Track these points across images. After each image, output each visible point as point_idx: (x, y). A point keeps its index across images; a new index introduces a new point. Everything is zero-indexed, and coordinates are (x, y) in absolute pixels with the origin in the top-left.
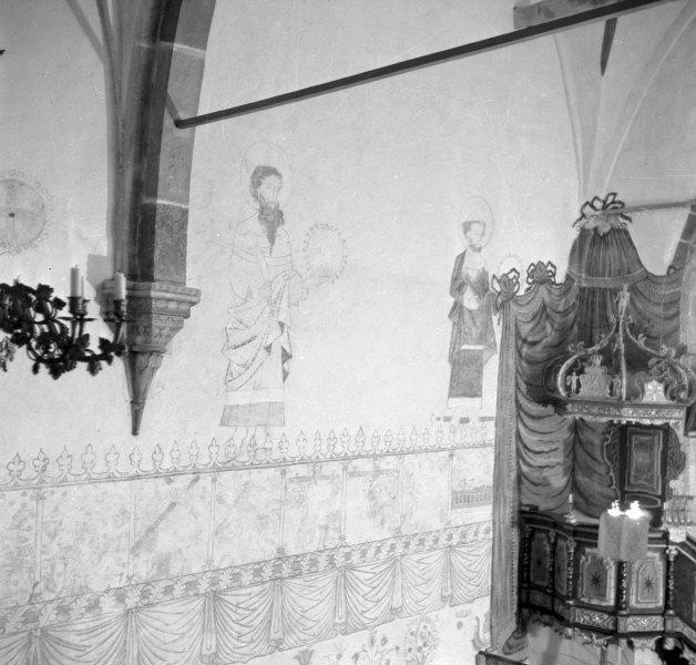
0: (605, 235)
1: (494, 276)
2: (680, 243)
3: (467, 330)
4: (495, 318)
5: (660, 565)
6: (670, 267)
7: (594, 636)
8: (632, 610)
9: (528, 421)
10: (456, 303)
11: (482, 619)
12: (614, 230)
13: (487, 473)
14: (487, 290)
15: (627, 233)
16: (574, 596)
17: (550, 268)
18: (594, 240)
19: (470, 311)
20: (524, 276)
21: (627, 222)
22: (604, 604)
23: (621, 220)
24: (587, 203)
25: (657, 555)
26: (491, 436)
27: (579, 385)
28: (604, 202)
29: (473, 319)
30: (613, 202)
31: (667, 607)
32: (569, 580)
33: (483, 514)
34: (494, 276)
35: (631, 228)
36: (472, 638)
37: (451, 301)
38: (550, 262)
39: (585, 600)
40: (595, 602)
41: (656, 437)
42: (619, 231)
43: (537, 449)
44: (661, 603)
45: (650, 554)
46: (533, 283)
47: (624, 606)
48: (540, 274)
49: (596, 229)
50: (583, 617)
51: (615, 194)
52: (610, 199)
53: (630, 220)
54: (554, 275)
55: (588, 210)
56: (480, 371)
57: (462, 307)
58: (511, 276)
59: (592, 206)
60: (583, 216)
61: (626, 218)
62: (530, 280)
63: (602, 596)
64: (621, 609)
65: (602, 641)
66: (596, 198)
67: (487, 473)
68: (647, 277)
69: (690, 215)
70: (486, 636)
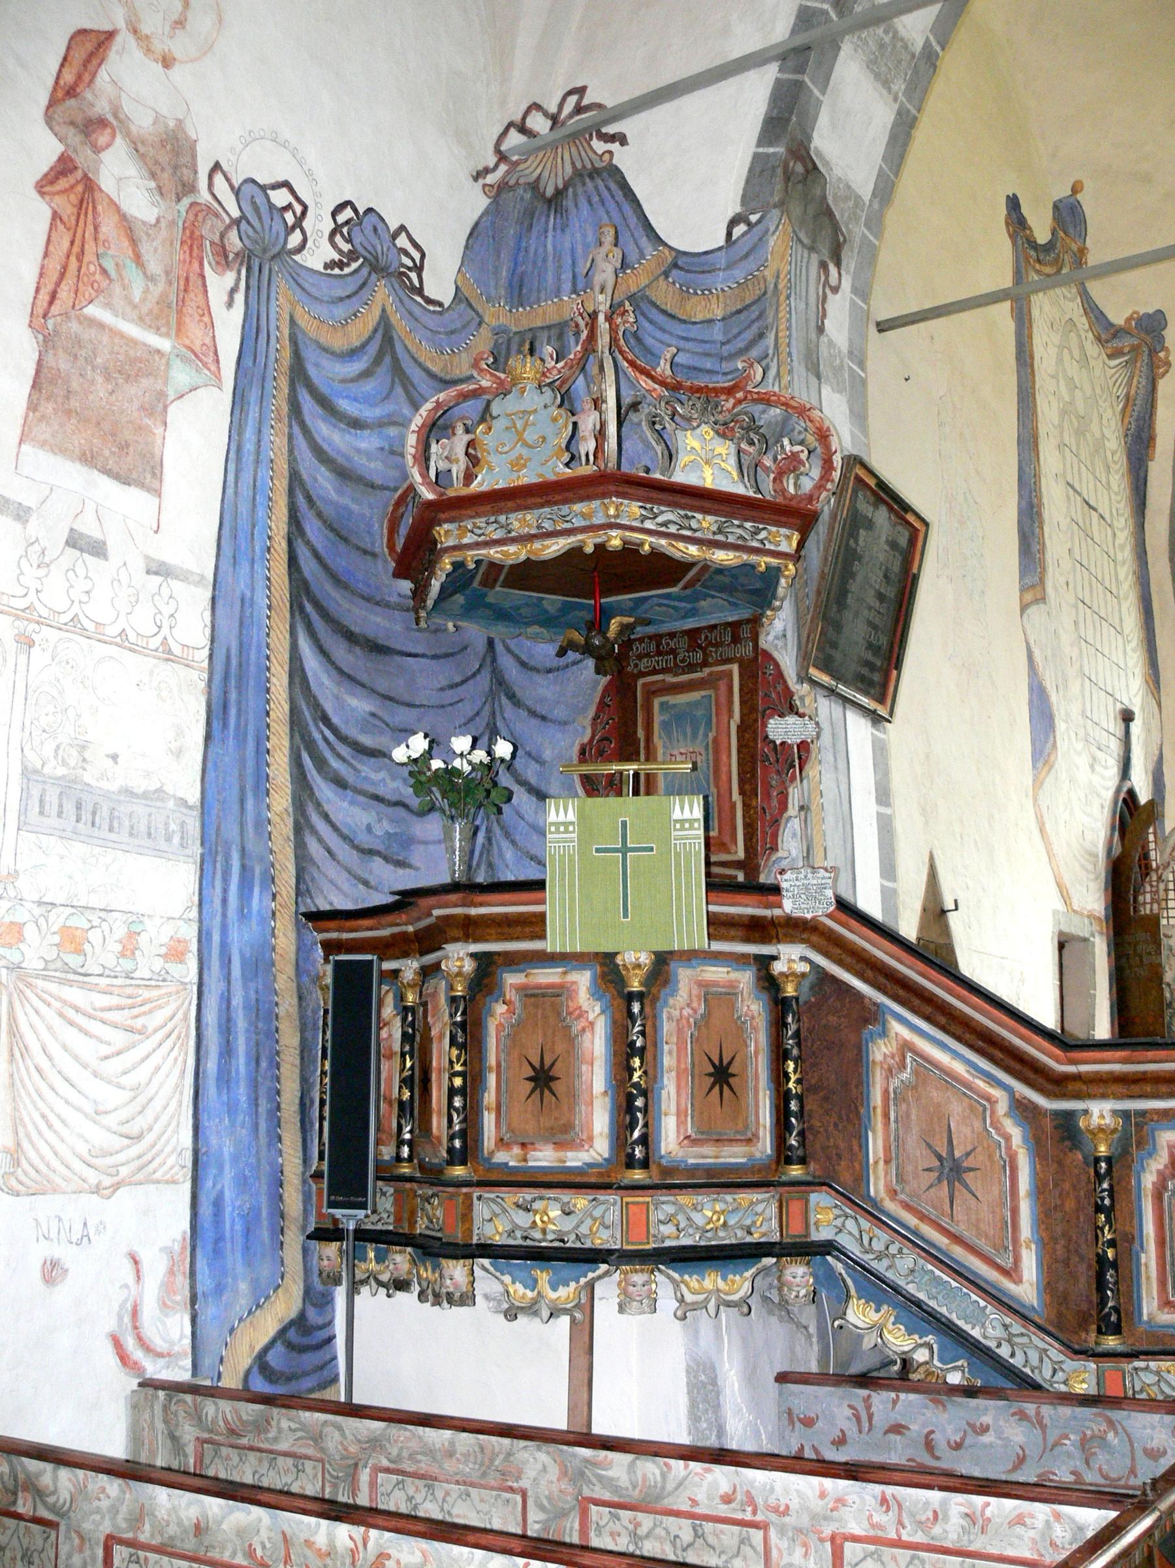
0: (559, 193)
1: (217, 167)
2: (756, 156)
3: (109, 265)
4: (219, 283)
5: (754, 1008)
6: (733, 223)
7: (543, 1278)
8: (667, 1171)
9: (340, 651)
10: (64, 167)
11: (156, 1268)
12: (582, 175)
13: (178, 753)
14: (189, 188)
15: (615, 173)
16: (467, 1148)
17: (402, 241)
18: (530, 214)
19: (123, 217)
20: (319, 223)
21: (615, 147)
22: (575, 1159)
23: (599, 146)
24: (511, 125)
25: (745, 978)
26: (193, 628)
27: (474, 461)
28: (555, 119)
29: (134, 242)
30: (579, 109)
31: (783, 1155)
32: (452, 1092)
33: (163, 891)
34: (217, 167)
35: (623, 158)
36: (111, 1325)
37: (47, 149)
38: (402, 228)
39: (508, 1158)
40: (544, 1157)
41: (722, 685)
42: (594, 173)
43: (366, 740)
44: (765, 1146)
45: (717, 973)
46: (352, 255)
47: (638, 1152)
48: (373, 251)
49: (534, 186)
50: (496, 1218)
51: (581, 91)
52: (572, 100)
53: (622, 139)
54: (419, 269)
55: (515, 139)
56: (157, 407)
57: (90, 186)
58: (280, 198)
59: (523, 129)
60: (502, 157)
61: (611, 138)
62: (346, 247)
63: (564, 1134)
64: (630, 1163)
65: (565, 1293)
66: (536, 106)
67: (178, 753)
68: (675, 265)
69: (778, 83)
70: (172, 1330)
